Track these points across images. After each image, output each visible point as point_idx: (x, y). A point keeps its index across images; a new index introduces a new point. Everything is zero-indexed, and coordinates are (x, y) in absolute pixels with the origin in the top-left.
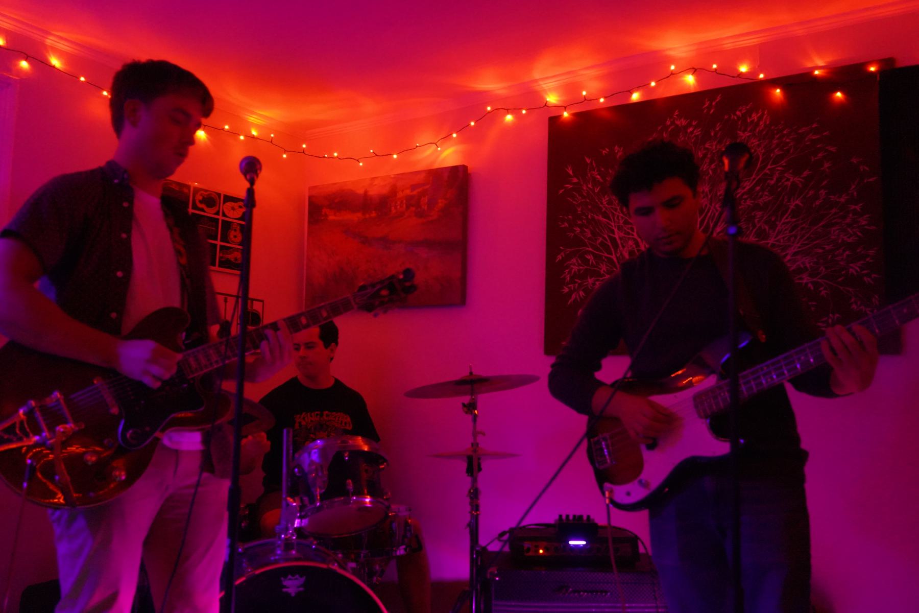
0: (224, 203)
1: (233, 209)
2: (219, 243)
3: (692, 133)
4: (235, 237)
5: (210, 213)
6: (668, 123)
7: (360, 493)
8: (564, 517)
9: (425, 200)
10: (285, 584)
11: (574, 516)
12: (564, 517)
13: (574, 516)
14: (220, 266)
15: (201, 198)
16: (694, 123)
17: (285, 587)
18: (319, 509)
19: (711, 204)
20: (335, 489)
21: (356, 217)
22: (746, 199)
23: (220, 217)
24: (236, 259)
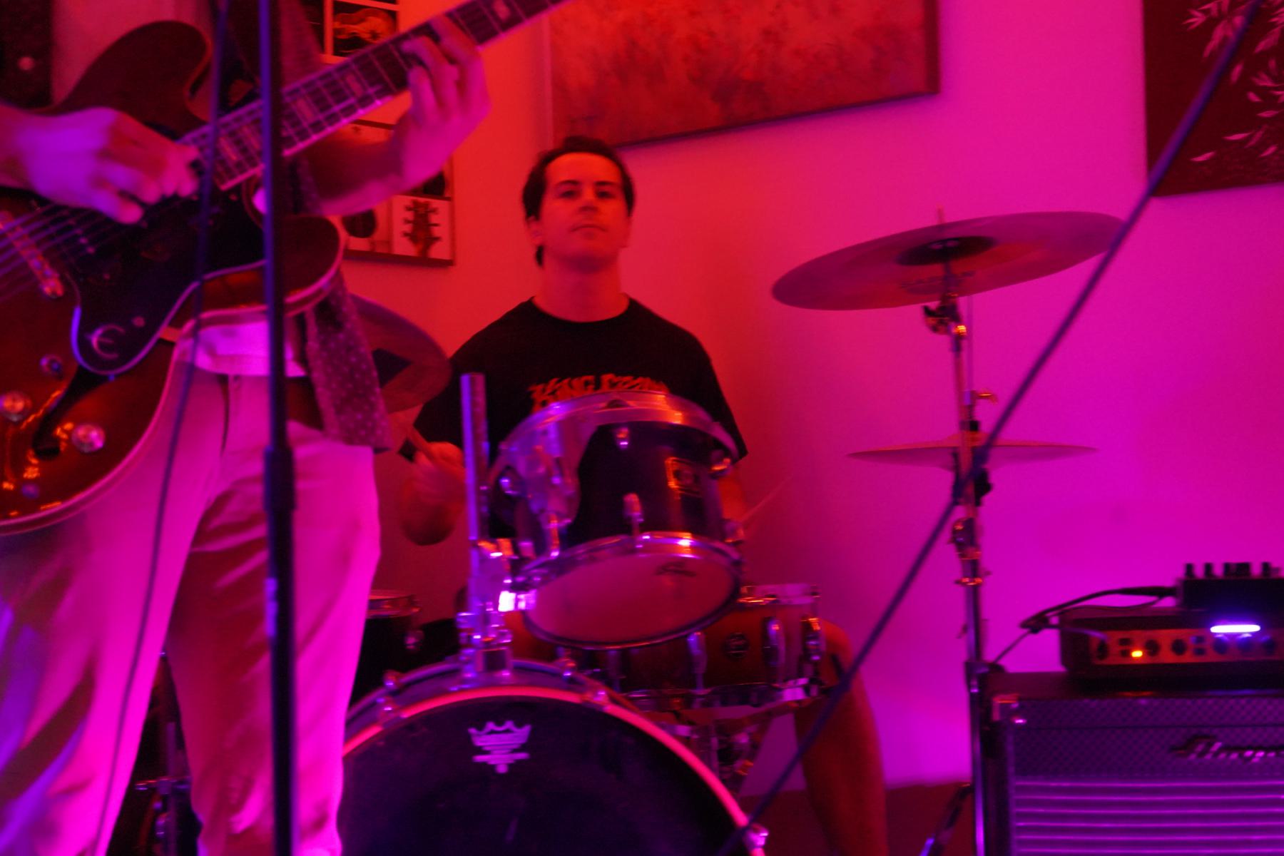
7: (659, 522)
8: (1199, 572)
10: (479, 742)
11: (1227, 567)
12: (1199, 572)
13: (1227, 567)
17: (480, 751)
18: (559, 567)
20: (595, 518)
24: (374, 35)
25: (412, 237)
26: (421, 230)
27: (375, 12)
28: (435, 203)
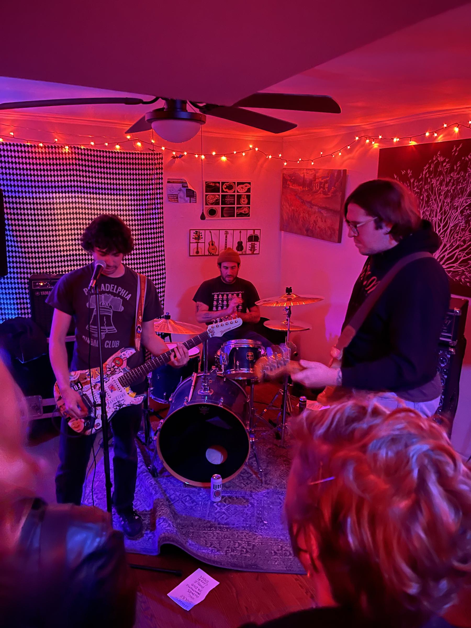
0: (237, 186)
1: (242, 188)
2: (236, 206)
3: (445, 166)
4: (244, 201)
5: (230, 193)
6: (434, 159)
9: (327, 185)
14: (237, 216)
15: (225, 187)
16: (447, 160)
19: (450, 210)
21: (300, 189)
22: (467, 209)
23: (236, 194)
24: (245, 212)
25: (251, 250)
26: (253, 248)
27: (245, 207)
28: (256, 243)
